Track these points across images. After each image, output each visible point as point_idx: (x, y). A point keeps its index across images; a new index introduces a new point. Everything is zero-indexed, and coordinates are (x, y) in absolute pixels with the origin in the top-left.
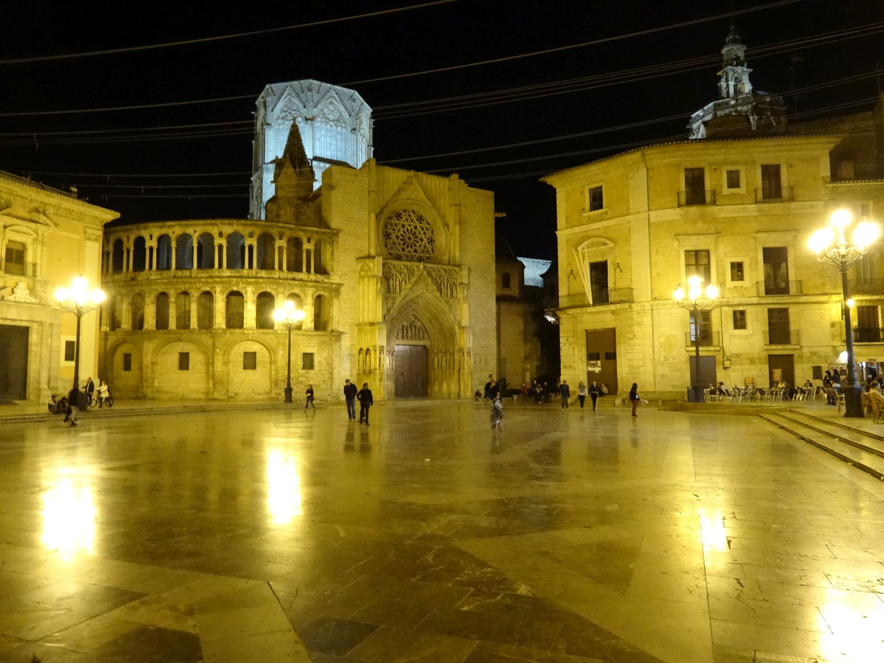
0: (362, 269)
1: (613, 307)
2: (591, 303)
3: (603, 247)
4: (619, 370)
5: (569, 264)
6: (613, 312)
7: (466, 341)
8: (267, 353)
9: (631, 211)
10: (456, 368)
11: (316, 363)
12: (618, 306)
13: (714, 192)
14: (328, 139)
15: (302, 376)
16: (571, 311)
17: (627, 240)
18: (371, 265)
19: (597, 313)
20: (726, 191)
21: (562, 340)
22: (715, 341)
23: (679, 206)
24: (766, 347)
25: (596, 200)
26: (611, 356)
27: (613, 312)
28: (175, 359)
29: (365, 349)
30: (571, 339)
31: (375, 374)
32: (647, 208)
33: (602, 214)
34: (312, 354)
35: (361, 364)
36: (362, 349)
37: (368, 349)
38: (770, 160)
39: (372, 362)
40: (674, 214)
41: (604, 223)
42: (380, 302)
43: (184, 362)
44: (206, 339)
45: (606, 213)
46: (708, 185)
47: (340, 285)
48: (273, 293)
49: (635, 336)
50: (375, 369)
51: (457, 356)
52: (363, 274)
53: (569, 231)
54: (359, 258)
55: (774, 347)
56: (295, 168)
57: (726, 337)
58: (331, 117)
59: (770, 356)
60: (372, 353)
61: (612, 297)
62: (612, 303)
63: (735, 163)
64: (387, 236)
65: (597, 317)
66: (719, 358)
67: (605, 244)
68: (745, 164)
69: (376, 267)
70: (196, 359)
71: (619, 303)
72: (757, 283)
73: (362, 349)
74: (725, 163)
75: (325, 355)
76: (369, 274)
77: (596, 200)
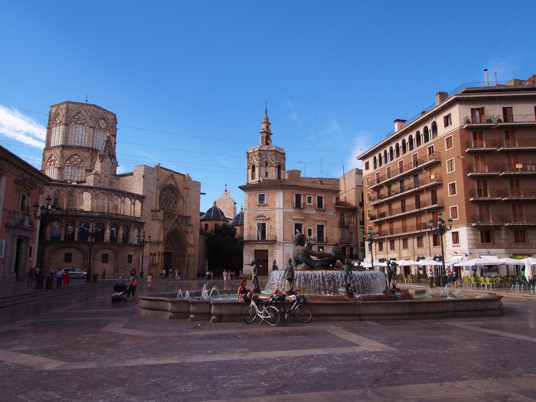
0: (153, 216)
5: (248, 223)
7: (191, 251)
8: (113, 255)
9: (276, 207)
10: (186, 263)
13: (304, 204)
14: (100, 137)
15: (127, 266)
17: (274, 218)
18: (158, 214)
20: (307, 204)
21: (244, 253)
28: (63, 256)
30: (248, 253)
31: (159, 266)
34: (131, 256)
35: (151, 261)
36: (151, 254)
38: (320, 195)
39: (157, 260)
40: (292, 210)
42: (162, 232)
43: (68, 258)
44: (85, 247)
46: (302, 201)
47: (145, 223)
48: (118, 224)
50: (159, 263)
51: (187, 258)
52: (153, 218)
56: (111, 159)
58: (103, 127)
60: (157, 257)
63: (310, 194)
64: (160, 200)
65: (261, 246)
68: (313, 195)
69: (161, 215)
70: (77, 256)
73: (151, 254)
74: (307, 194)
75: (137, 256)
76: (157, 218)
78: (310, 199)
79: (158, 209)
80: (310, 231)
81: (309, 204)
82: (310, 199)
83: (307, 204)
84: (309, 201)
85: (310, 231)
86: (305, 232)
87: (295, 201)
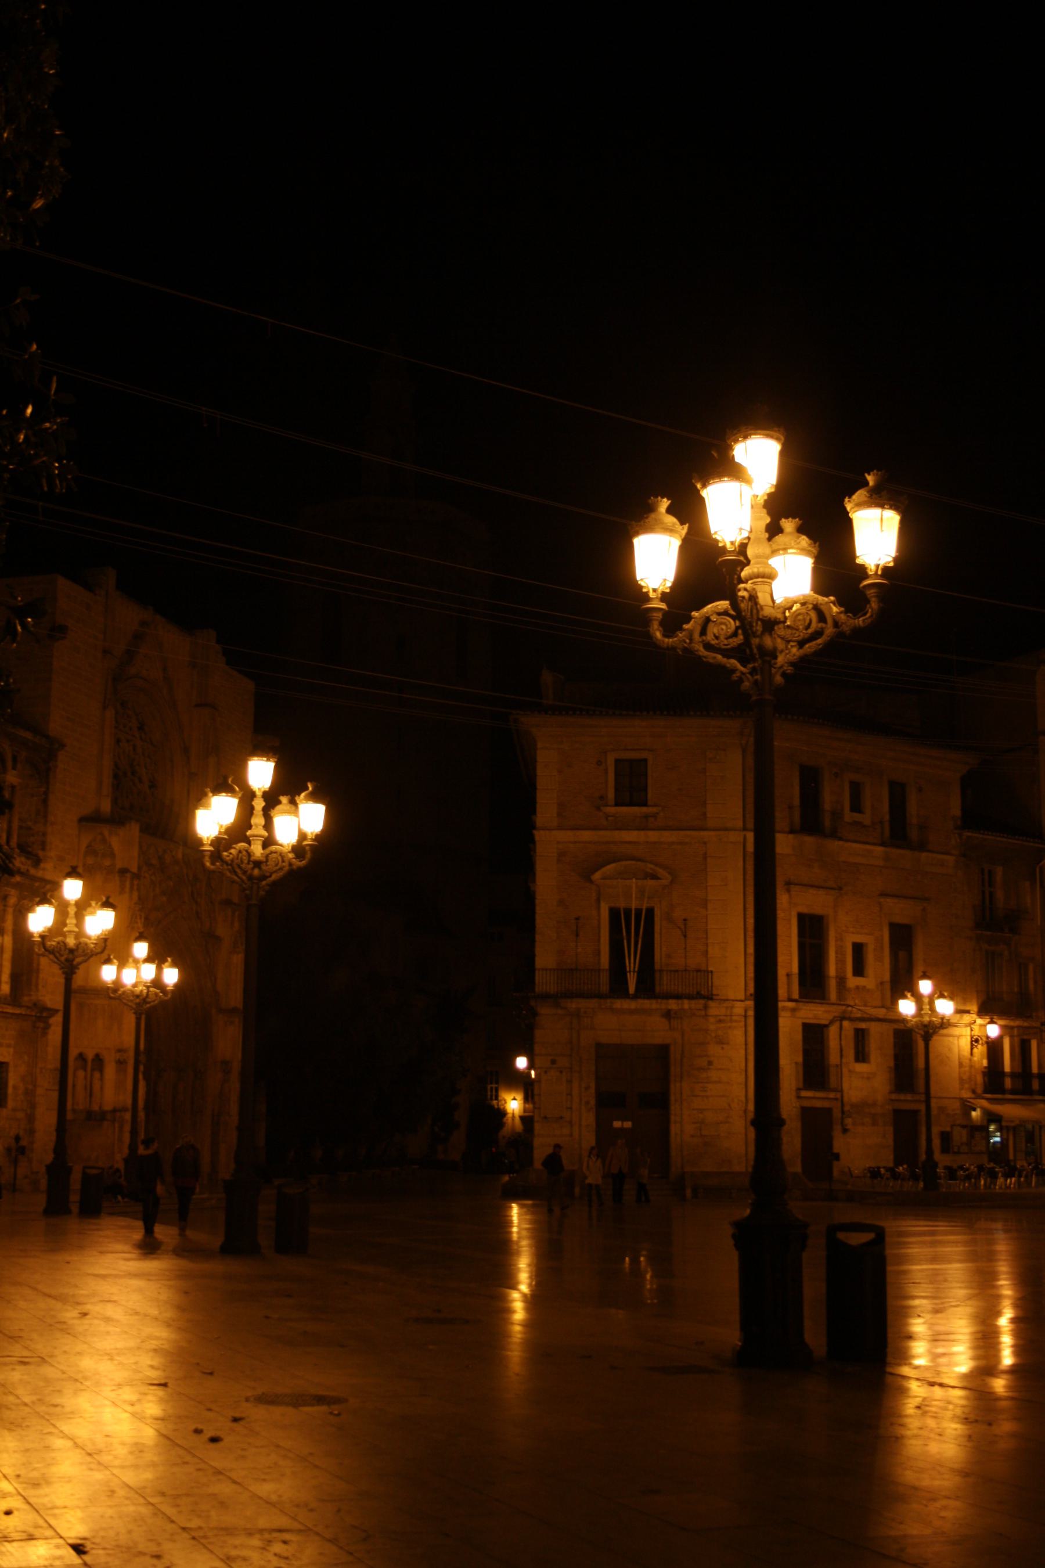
0: (90, 851)
1: (673, 1005)
2: (632, 989)
3: (651, 883)
4: (674, 1129)
6: (668, 1015)
11: (10, 1090)
12: (686, 1004)
16: (573, 1005)
18: (115, 842)
19: (632, 1012)
20: (848, 816)
22: (833, 1081)
23: (791, 832)
24: (894, 1096)
25: (632, 784)
26: (659, 1102)
27: (668, 1015)
29: (90, 1055)
32: (740, 824)
33: (646, 817)
37: (97, 1055)
41: (653, 836)
45: (655, 816)
49: (710, 1063)
53: (567, 835)
54: (82, 820)
55: (902, 1097)
57: (845, 1070)
59: (897, 1112)
61: (665, 983)
62: (668, 996)
66: (837, 1114)
67: (654, 877)
71: (690, 997)
72: (882, 983)
77: (632, 784)
78: (856, 789)
79: (106, 806)
80: (858, 950)
81: (857, 817)
82: (856, 789)
83: (848, 816)
84: (856, 807)
85: (858, 950)
86: (841, 962)
87: (797, 802)
